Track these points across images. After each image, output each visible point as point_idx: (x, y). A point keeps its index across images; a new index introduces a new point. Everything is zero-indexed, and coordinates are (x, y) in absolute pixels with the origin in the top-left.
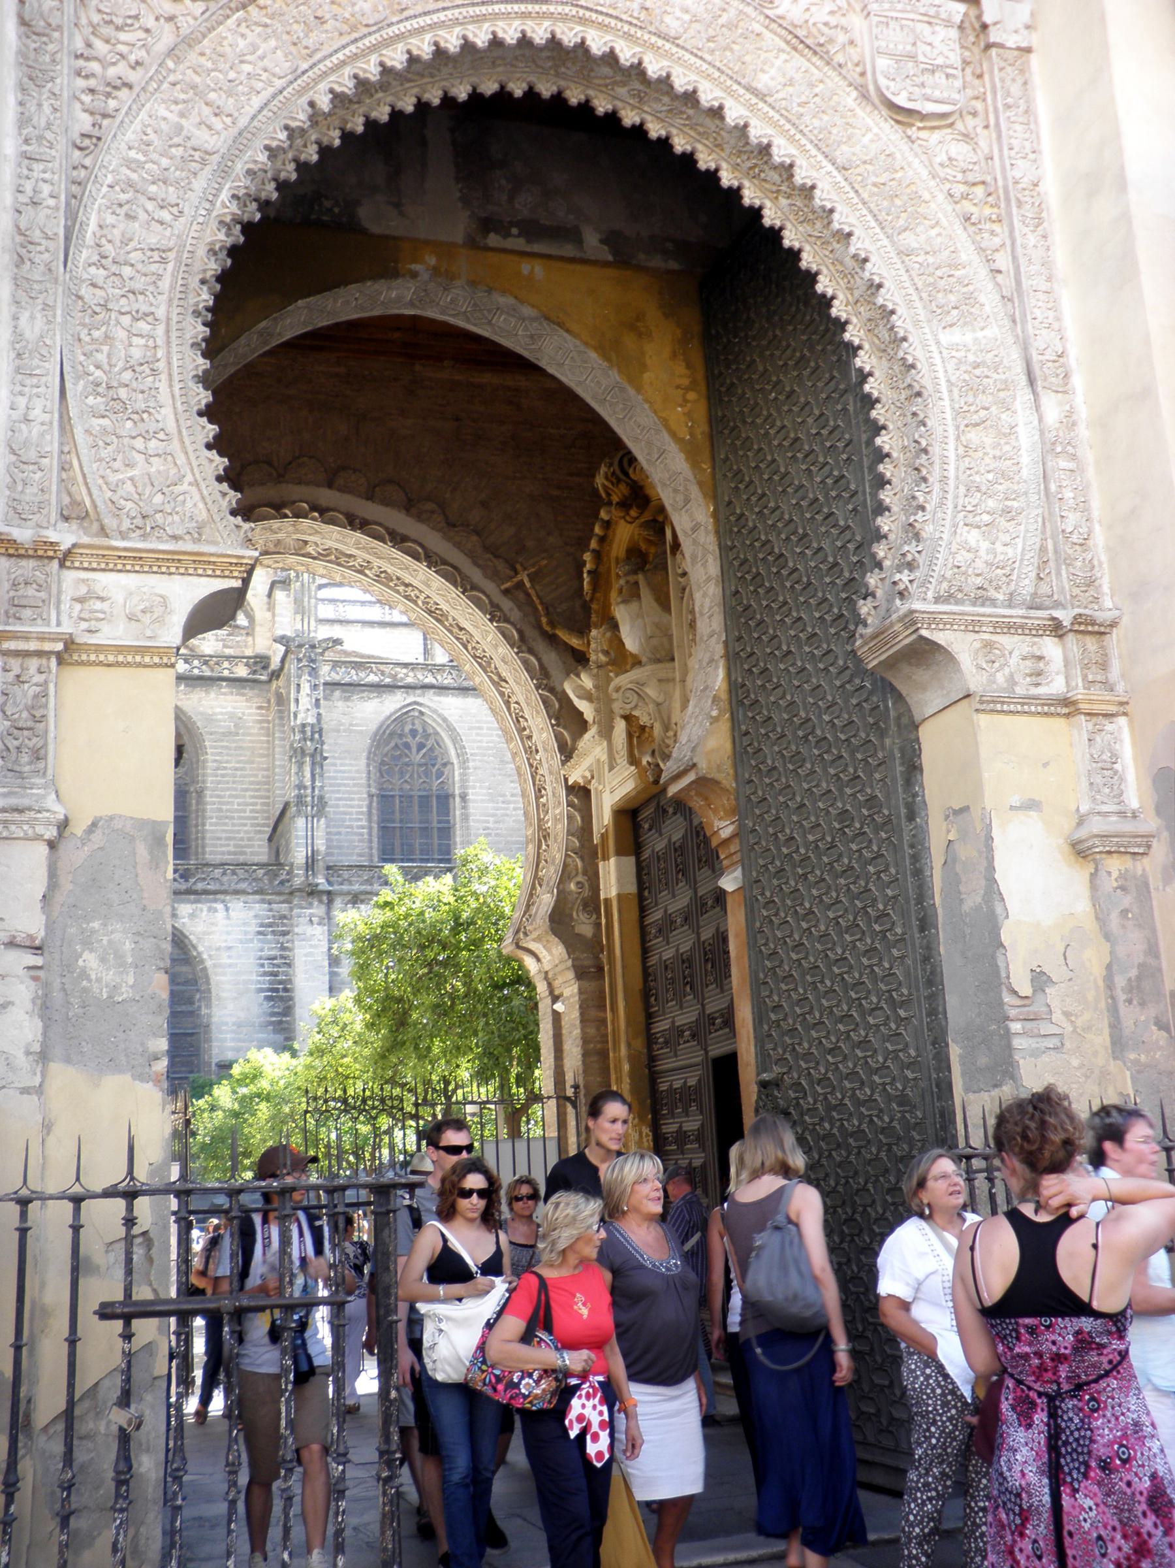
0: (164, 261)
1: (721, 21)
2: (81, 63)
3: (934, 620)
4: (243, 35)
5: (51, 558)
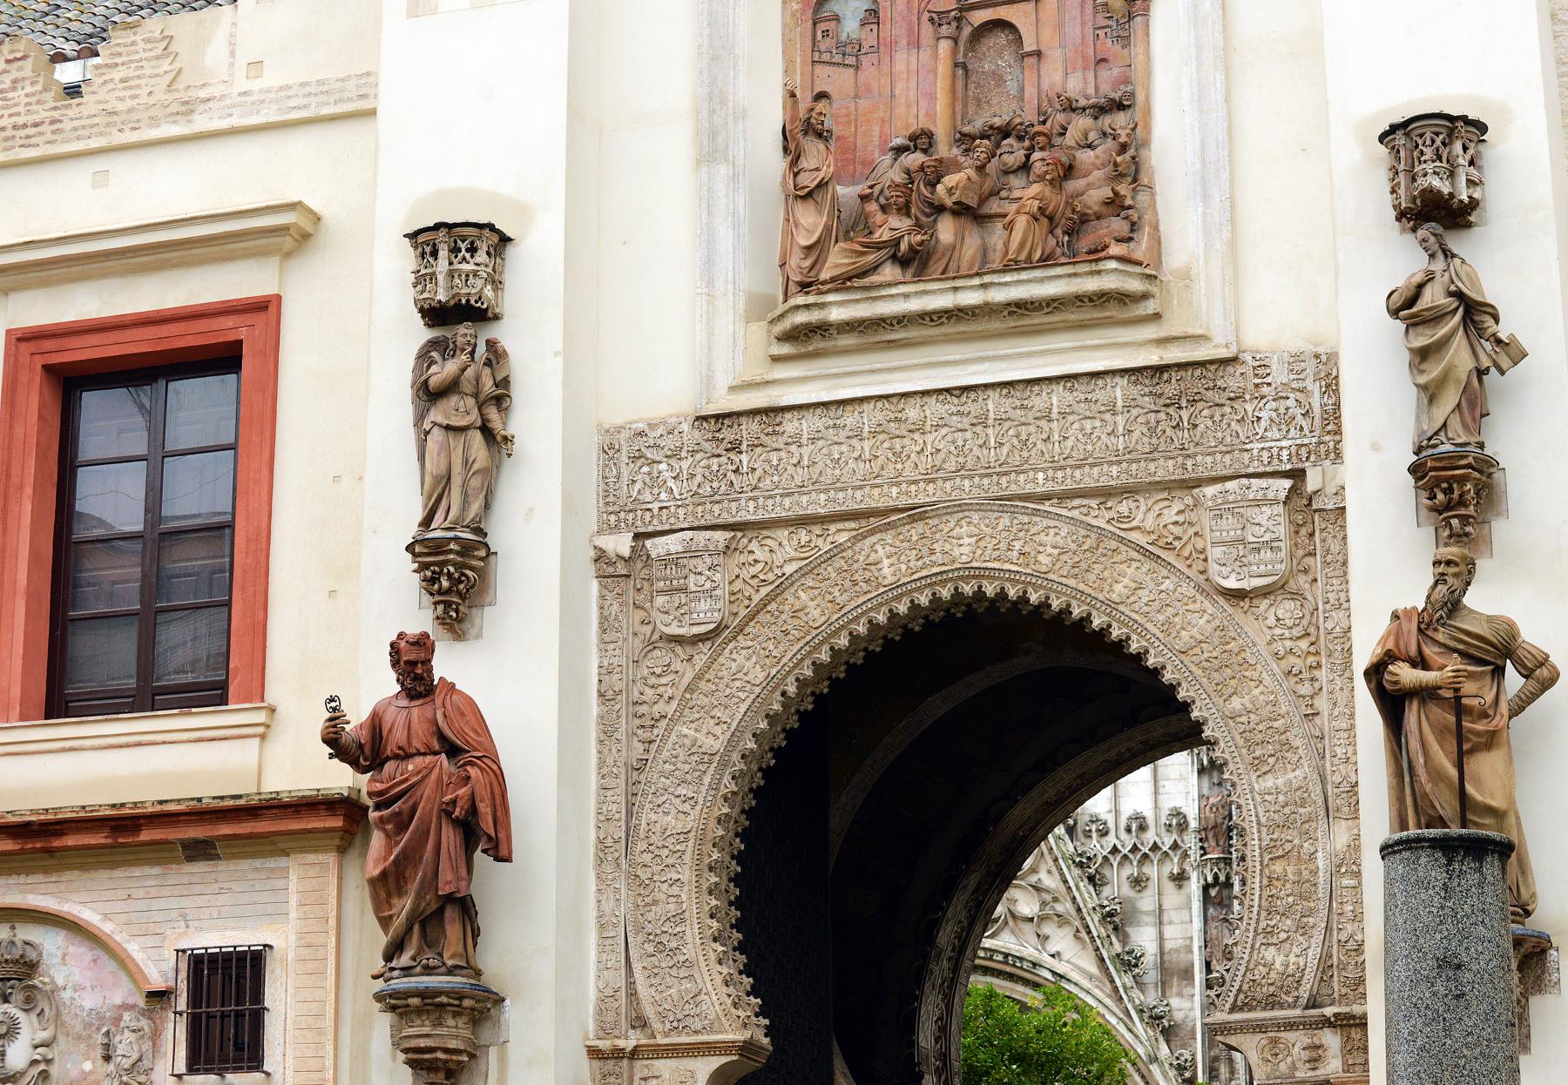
0: (686, 840)
1: (1085, 547)
2: (638, 708)
4: (734, 660)
5: (622, 1058)
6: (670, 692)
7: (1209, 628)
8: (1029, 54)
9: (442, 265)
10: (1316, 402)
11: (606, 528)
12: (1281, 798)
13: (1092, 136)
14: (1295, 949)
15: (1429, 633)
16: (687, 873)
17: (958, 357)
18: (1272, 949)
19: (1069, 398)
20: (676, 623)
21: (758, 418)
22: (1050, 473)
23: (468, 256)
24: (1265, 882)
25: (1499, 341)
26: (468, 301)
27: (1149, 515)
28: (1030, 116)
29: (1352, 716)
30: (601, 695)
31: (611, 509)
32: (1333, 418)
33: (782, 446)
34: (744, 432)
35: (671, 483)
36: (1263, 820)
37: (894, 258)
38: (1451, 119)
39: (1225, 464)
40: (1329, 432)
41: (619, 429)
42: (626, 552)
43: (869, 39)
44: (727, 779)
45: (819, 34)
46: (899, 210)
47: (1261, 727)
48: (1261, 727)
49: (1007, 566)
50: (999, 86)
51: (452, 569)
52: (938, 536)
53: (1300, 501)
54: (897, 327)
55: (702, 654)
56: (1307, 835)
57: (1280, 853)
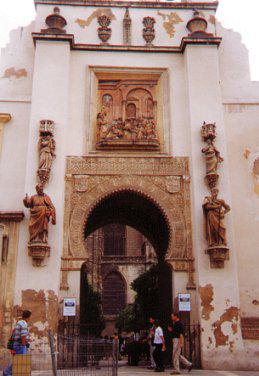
27: (157, 179)
32: (187, 169)
53: (182, 180)
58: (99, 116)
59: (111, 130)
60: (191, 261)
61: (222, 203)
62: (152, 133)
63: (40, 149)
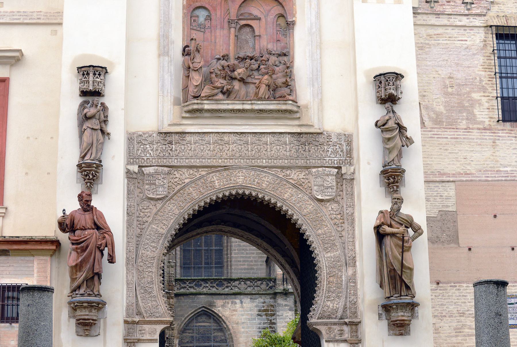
0: (154, 259)
1: (276, 183)
3: (317, 324)
6: (149, 214)
7: (312, 209)
8: (257, 36)
9: (91, 77)
10: (345, 148)
11: (129, 163)
12: (332, 259)
13: (277, 63)
14: (336, 302)
15: (393, 218)
16: (154, 269)
17: (240, 123)
18: (329, 302)
19: (273, 139)
20: (152, 194)
21: (178, 135)
22: (267, 160)
23: (98, 76)
24: (327, 283)
25: (407, 138)
26: (98, 90)
27: (295, 175)
28: (257, 54)
29: (354, 238)
30: (128, 213)
31: (131, 158)
32: (349, 153)
33: (185, 144)
34: (173, 139)
35: (150, 152)
36: (327, 265)
37: (221, 92)
38: (397, 74)
39: (319, 163)
40: (348, 157)
41: (134, 133)
42: (136, 171)
43: (208, 24)
44: (166, 242)
45: (192, 21)
46: (223, 78)
47: (326, 239)
48: (326, 239)
49: (253, 186)
50: (247, 44)
51: (94, 172)
52: (232, 175)
53: (340, 176)
54: (223, 112)
55: (159, 205)
56: (340, 271)
57: (332, 275)
58: (186, 52)
59: (208, 80)
60: (355, 325)
61: (409, 223)
62: (286, 84)
63: (81, 124)
